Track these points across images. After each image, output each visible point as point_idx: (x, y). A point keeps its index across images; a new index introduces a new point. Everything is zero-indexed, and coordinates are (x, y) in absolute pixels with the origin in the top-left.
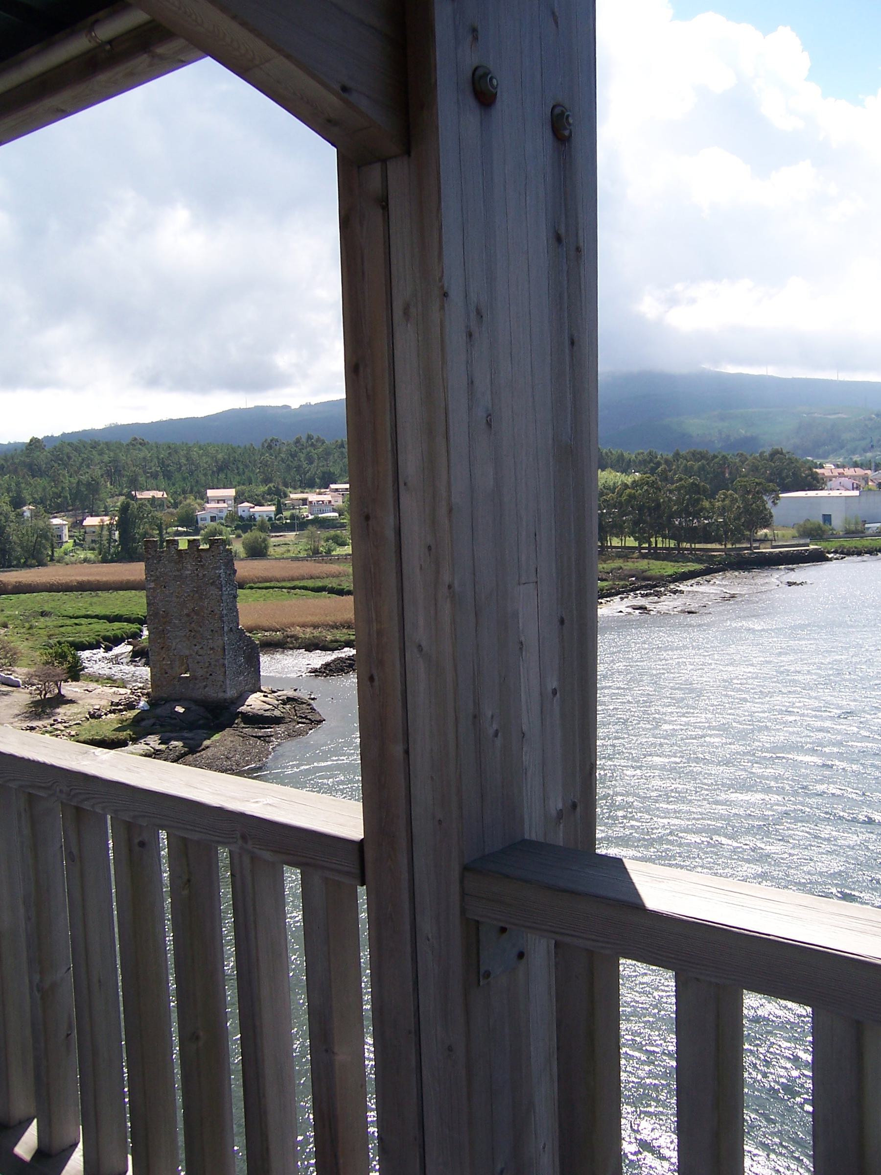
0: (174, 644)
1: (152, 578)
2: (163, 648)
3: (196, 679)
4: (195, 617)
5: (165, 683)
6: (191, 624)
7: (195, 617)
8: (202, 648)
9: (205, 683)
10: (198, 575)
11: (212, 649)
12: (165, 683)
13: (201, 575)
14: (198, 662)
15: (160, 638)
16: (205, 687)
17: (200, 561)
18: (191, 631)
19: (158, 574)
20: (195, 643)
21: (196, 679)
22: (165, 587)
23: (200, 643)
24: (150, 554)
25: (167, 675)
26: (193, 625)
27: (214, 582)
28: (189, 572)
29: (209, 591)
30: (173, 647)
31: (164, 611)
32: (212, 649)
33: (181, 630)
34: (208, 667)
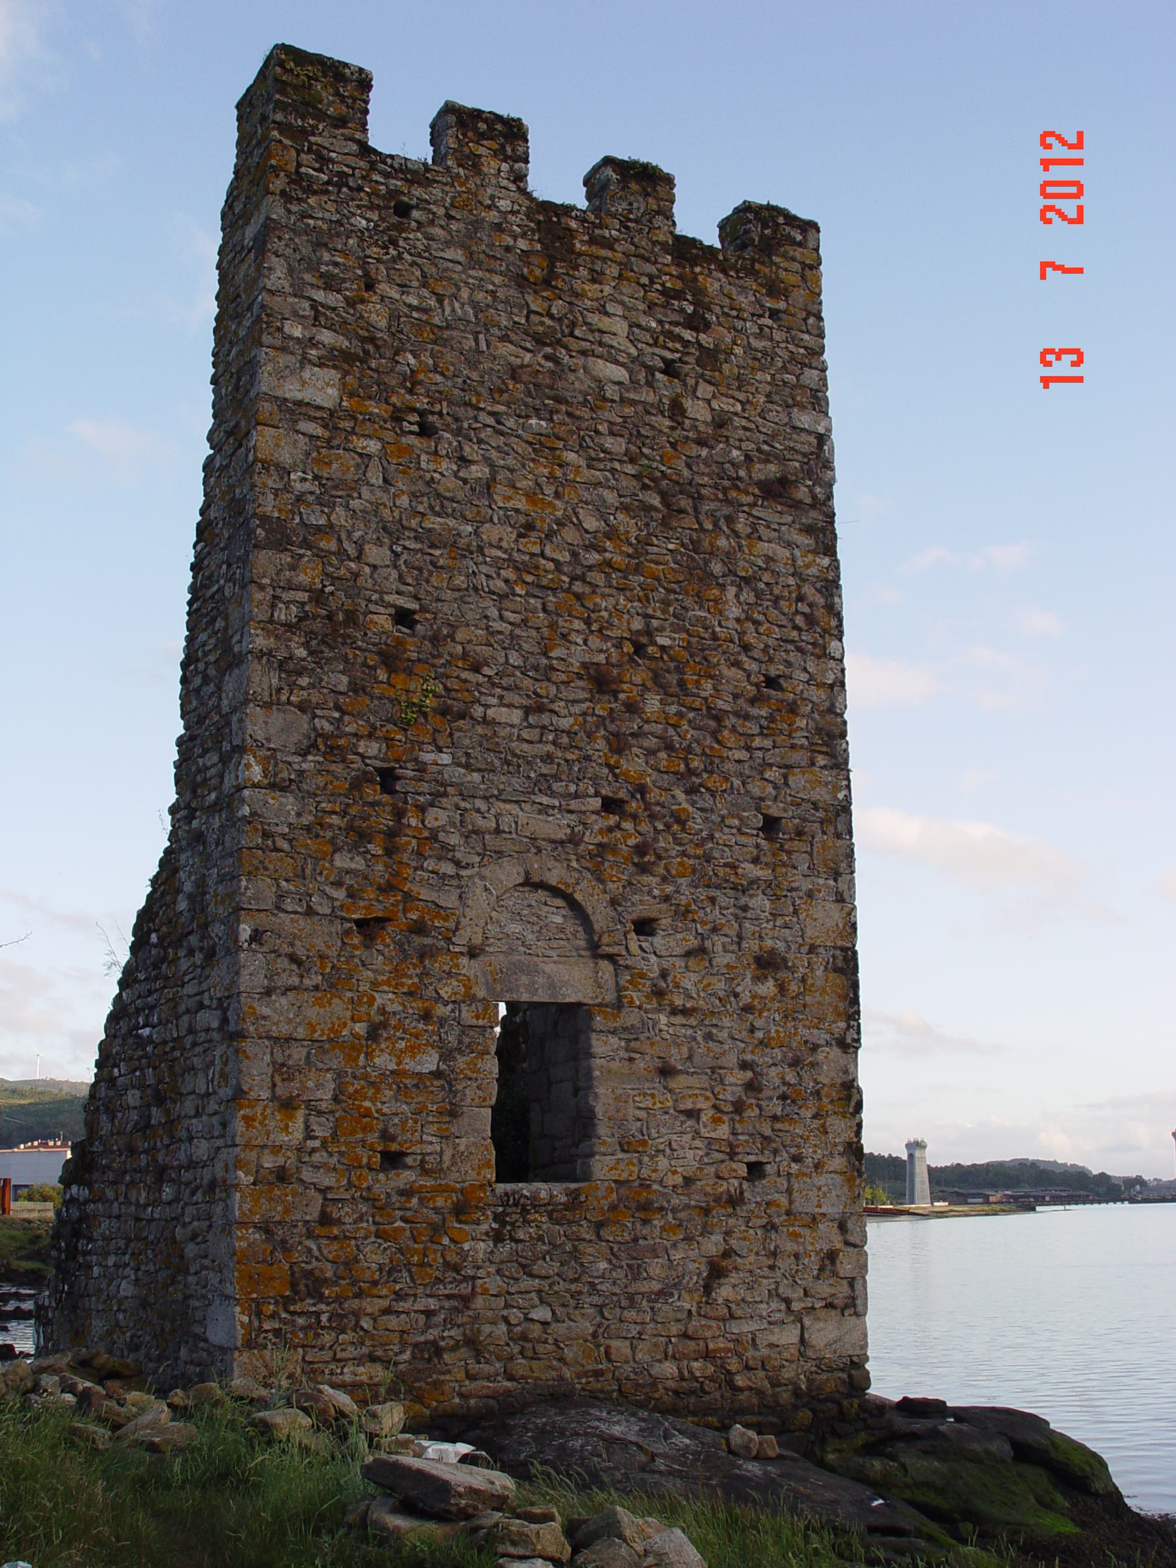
0: (479, 900)
1: (326, 337)
2: (369, 928)
3: (646, 1208)
4: (653, 703)
5: (374, 1257)
6: (618, 744)
7: (653, 703)
8: (700, 952)
9: (713, 1245)
10: (677, 410)
11: (767, 963)
12: (374, 1257)
13: (697, 410)
14: (666, 1071)
15: (359, 837)
16: (716, 1272)
17: (697, 323)
18: (610, 805)
19: (377, 316)
20: (642, 906)
21: (646, 1208)
22: (425, 431)
23: (684, 913)
24: (323, 161)
25: (386, 1184)
26: (634, 764)
27: (783, 482)
28: (621, 374)
29: (754, 535)
30: (469, 934)
31: (403, 617)
32: (767, 963)
33: (543, 783)
34: (739, 1107)
